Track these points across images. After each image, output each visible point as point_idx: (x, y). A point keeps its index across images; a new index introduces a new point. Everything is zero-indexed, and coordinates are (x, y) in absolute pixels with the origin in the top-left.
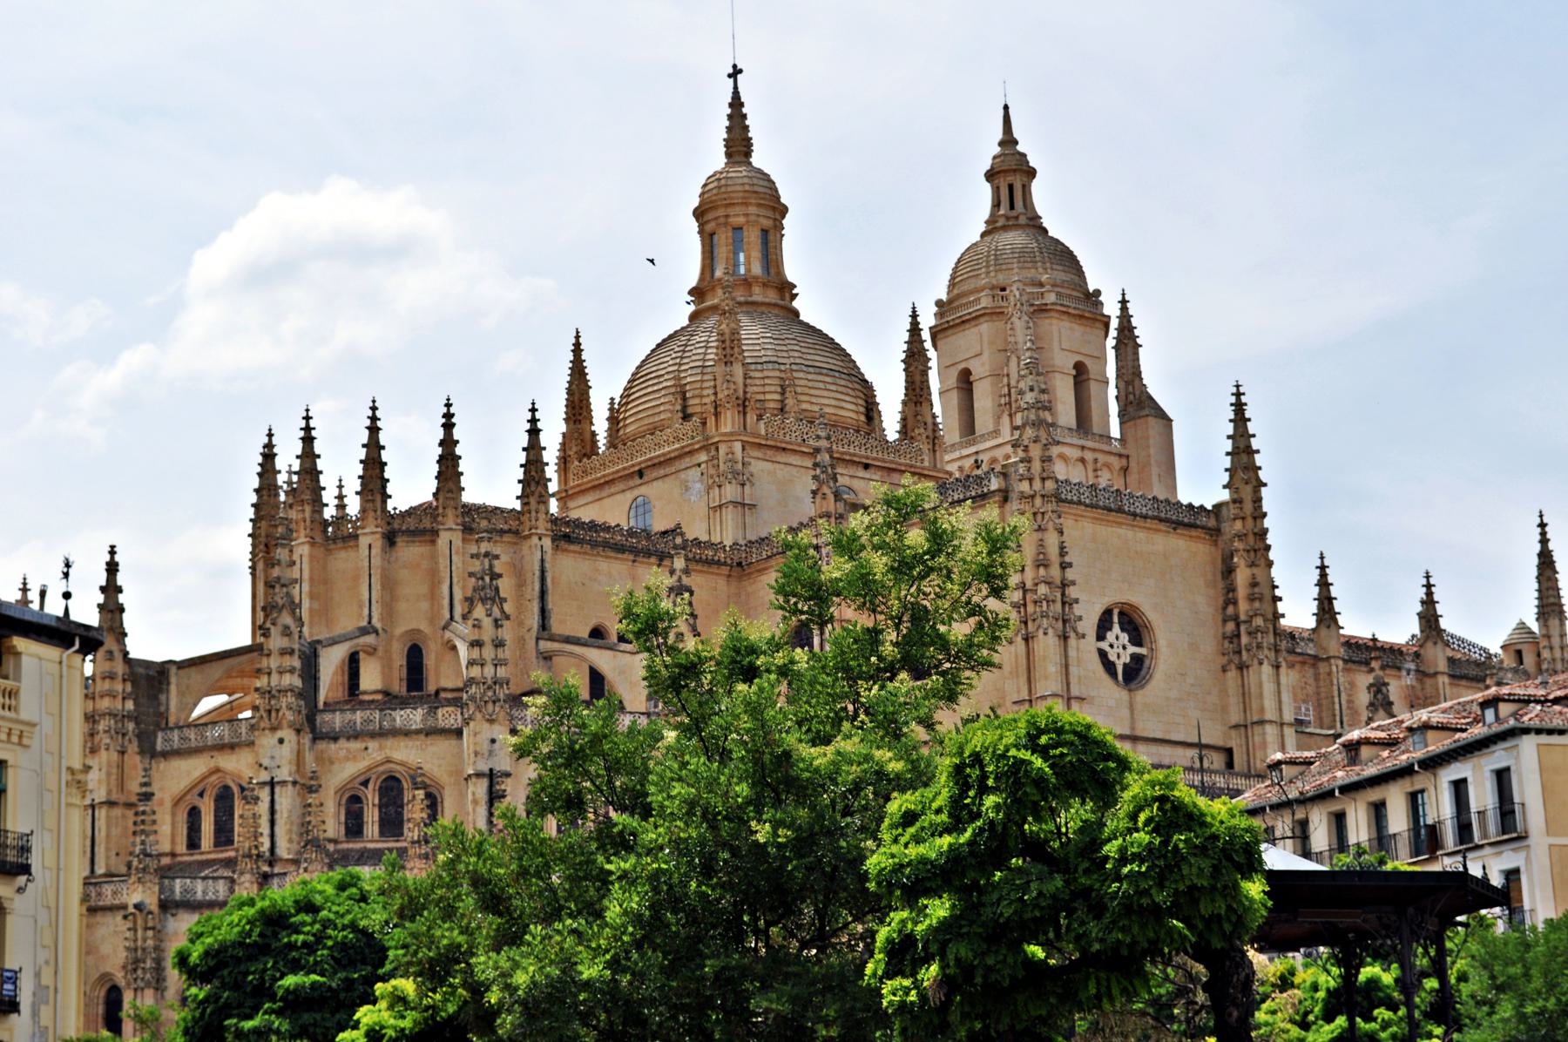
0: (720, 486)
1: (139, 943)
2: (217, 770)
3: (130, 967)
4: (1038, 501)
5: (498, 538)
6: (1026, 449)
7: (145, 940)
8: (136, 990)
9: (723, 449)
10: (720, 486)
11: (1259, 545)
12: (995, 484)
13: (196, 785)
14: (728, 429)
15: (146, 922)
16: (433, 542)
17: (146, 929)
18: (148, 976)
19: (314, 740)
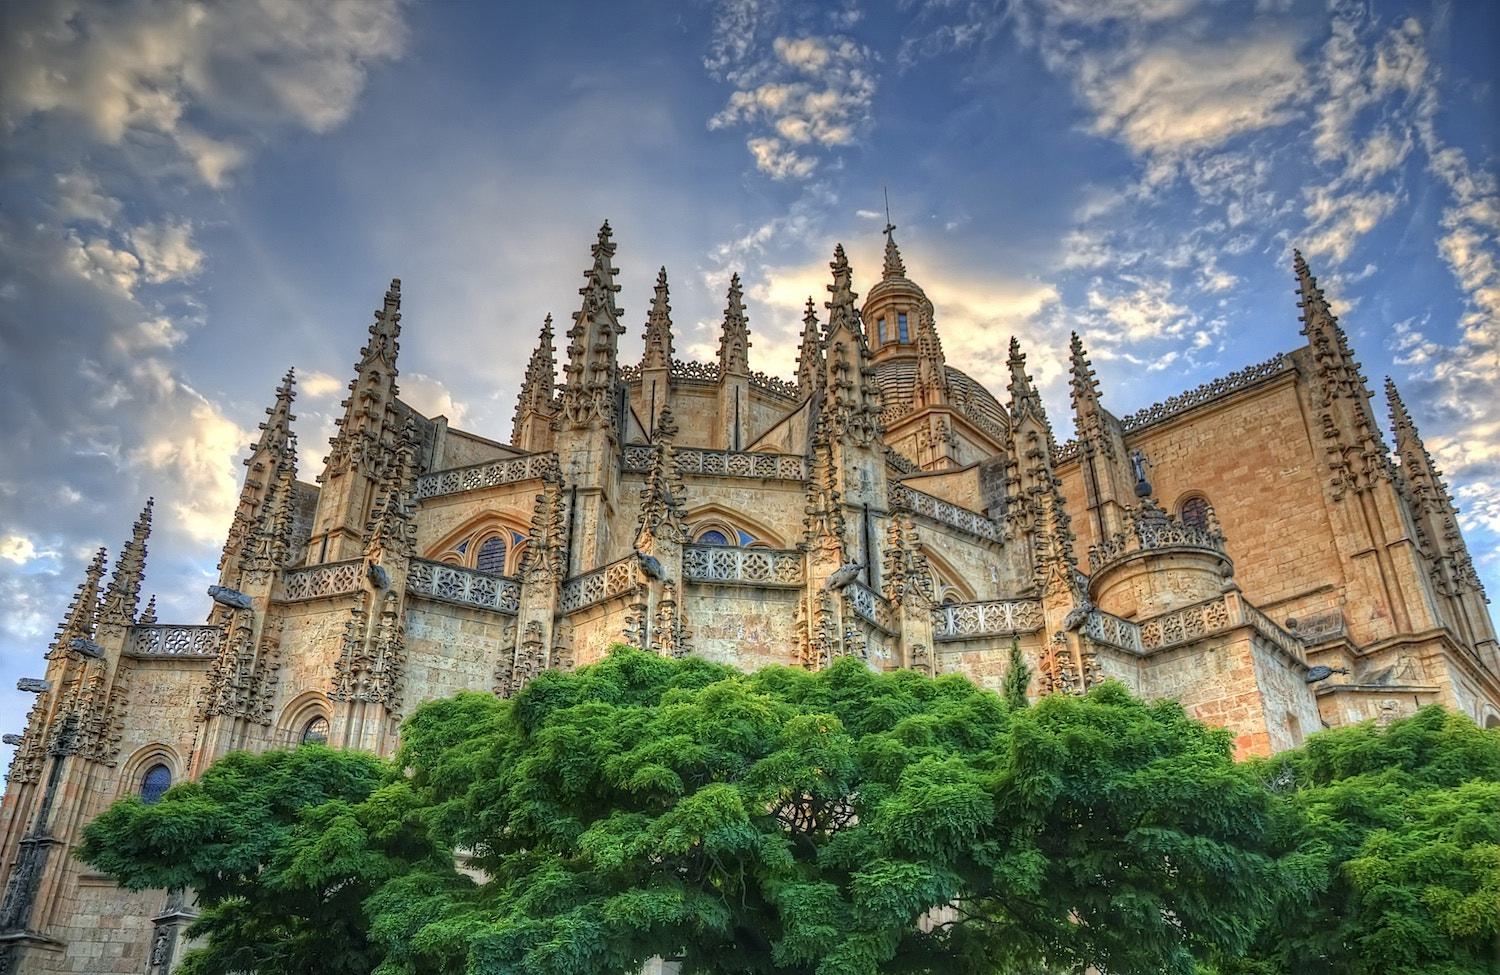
0: (932, 447)
1: (368, 635)
2: (490, 516)
3: (348, 668)
4: (1343, 373)
5: (778, 402)
6: (1319, 332)
7: (378, 630)
8: (353, 702)
9: (933, 419)
10: (932, 447)
11: (1441, 496)
12: (1289, 365)
13: (457, 536)
14: (938, 403)
15: (385, 605)
16: (715, 394)
17: (388, 614)
18: (376, 683)
19: (622, 472)
